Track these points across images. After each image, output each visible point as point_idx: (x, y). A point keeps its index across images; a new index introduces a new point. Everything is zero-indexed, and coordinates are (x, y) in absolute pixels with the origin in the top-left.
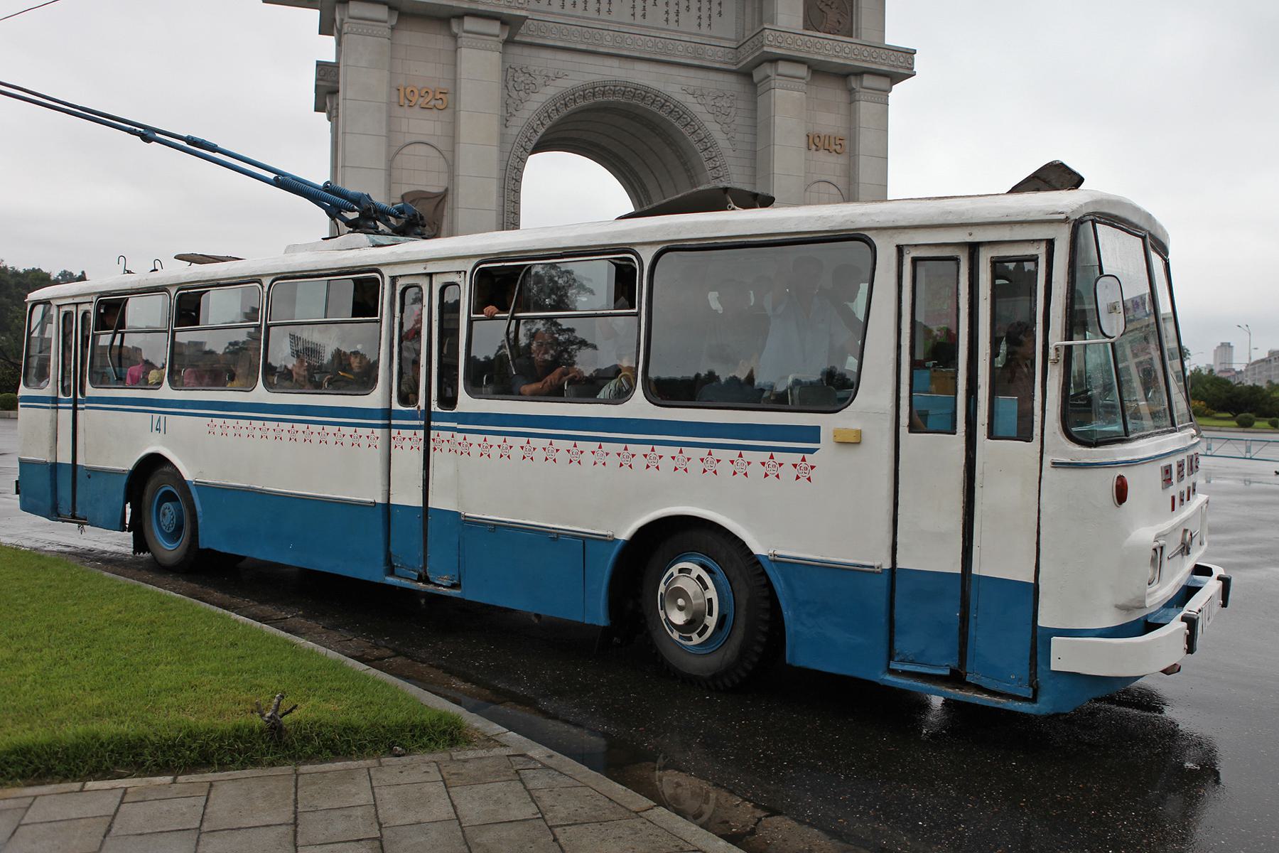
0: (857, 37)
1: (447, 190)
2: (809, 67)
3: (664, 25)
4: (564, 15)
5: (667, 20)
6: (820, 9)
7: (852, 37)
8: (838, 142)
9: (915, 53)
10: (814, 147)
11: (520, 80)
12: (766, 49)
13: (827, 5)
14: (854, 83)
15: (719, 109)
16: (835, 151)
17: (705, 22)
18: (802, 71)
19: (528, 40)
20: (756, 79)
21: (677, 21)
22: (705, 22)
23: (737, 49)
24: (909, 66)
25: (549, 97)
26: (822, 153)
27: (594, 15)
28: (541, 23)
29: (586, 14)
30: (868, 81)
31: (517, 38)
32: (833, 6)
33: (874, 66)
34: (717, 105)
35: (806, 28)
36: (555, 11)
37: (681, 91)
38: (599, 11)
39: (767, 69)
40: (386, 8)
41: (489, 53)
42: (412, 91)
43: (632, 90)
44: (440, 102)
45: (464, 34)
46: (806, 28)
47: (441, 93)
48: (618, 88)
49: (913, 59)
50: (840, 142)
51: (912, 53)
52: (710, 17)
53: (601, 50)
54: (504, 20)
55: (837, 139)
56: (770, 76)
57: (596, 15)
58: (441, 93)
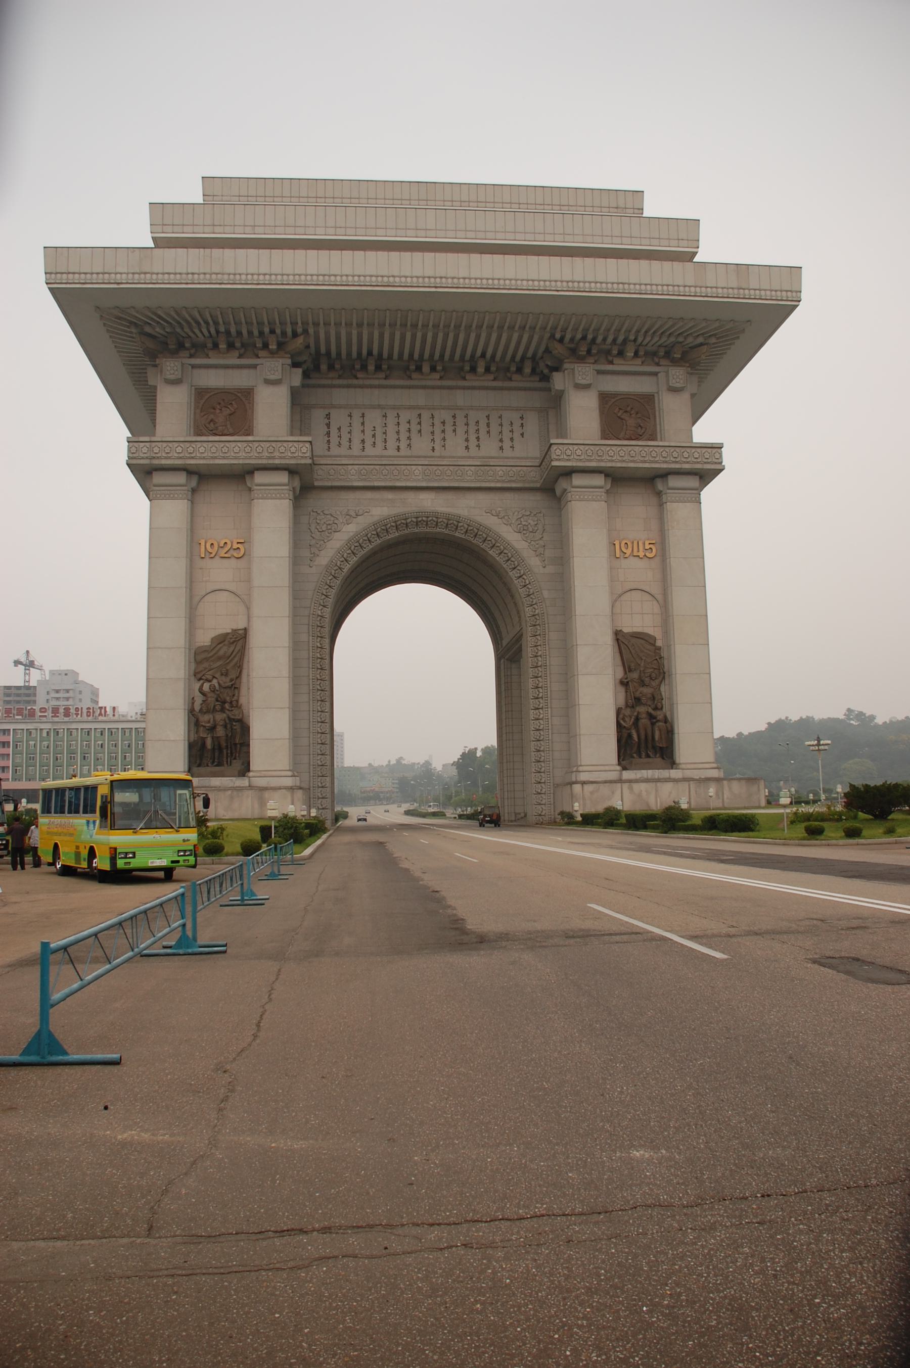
0: (661, 440)
1: (245, 629)
2: (607, 475)
3: (465, 453)
4: (366, 456)
5: (467, 448)
6: (619, 418)
7: (656, 440)
8: (647, 547)
9: (721, 448)
10: (622, 554)
11: (322, 522)
12: (555, 463)
13: (626, 412)
14: (660, 485)
15: (525, 528)
16: (645, 555)
17: (507, 444)
18: (599, 480)
19: (329, 484)
20: (558, 492)
21: (478, 446)
22: (507, 444)
23: (540, 466)
24: (716, 461)
25: (352, 534)
26: (633, 562)
27: (391, 452)
28: (340, 467)
29: (385, 453)
30: (673, 482)
31: (316, 484)
32: (632, 412)
33: (677, 466)
34: (524, 523)
35: (604, 437)
36: (355, 454)
37: (485, 514)
38: (398, 449)
39: (562, 484)
40: (184, 474)
41: (278, 501)
42: (212, 544)
43: (434, 519)
44: (238, 551)
45: (256, 487)
46: (604, 437)
47: (238, 543)
48: (410, 520)
49: (721, 454)
50: (651, 546)
51: (719, 447)
52: (512, 439)
53: (398, 484)
54: (292, 471)
55: (647, 543)
56: (565, 490)
57: (396, 453)
58: (238, 543)
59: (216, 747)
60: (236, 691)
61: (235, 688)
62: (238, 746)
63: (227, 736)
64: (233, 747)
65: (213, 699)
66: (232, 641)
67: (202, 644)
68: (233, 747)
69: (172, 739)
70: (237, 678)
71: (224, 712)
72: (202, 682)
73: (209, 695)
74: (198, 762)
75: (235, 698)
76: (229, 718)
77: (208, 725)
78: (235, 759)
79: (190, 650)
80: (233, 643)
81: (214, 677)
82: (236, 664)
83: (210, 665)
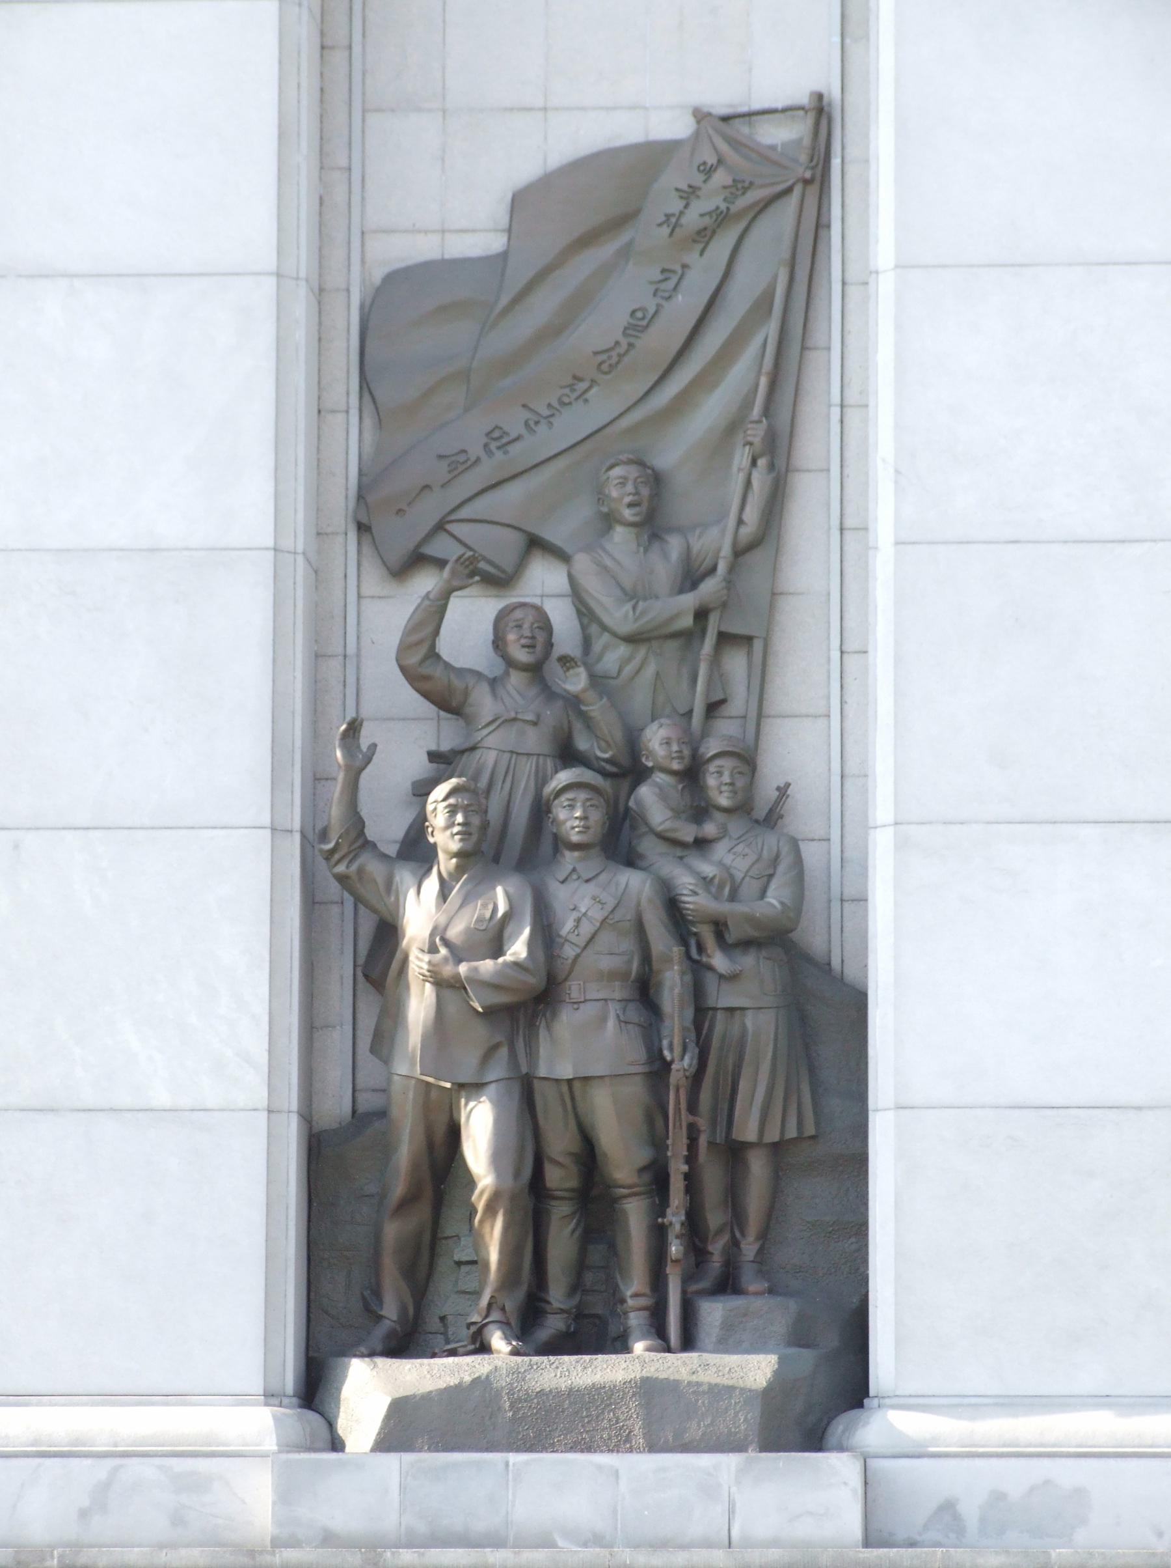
59: (558, 1178)
60: (736, 663)
61: (725, 639)
62: (758, 1167)
63: (658, 1070)
64: (713, 1178)
65: (535, 740)
66: (693, 218)
67: (425, 249)
68: (713, 1178)
69: (161, 1097)
70: (740, 552)
71: (631, 860)
72: (426, 583)
73: (485, 705)
74: (390, 1310)
75: (726, 729)
76: (672, 906)
77: (487, 966)
78: (728, 1284)
79: (320, 293)
80: (704, 236)
81: (535, 544)
82: (733, 427)
83: (498, 439)
